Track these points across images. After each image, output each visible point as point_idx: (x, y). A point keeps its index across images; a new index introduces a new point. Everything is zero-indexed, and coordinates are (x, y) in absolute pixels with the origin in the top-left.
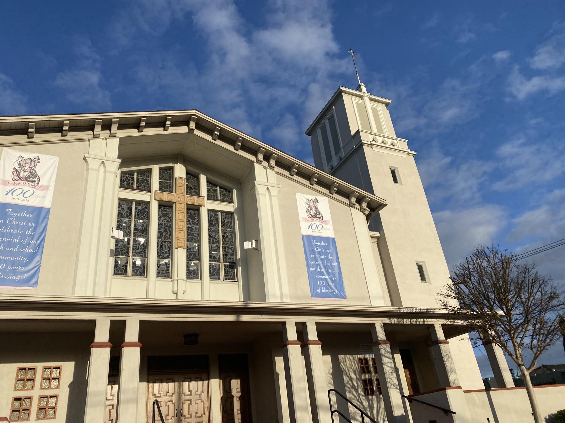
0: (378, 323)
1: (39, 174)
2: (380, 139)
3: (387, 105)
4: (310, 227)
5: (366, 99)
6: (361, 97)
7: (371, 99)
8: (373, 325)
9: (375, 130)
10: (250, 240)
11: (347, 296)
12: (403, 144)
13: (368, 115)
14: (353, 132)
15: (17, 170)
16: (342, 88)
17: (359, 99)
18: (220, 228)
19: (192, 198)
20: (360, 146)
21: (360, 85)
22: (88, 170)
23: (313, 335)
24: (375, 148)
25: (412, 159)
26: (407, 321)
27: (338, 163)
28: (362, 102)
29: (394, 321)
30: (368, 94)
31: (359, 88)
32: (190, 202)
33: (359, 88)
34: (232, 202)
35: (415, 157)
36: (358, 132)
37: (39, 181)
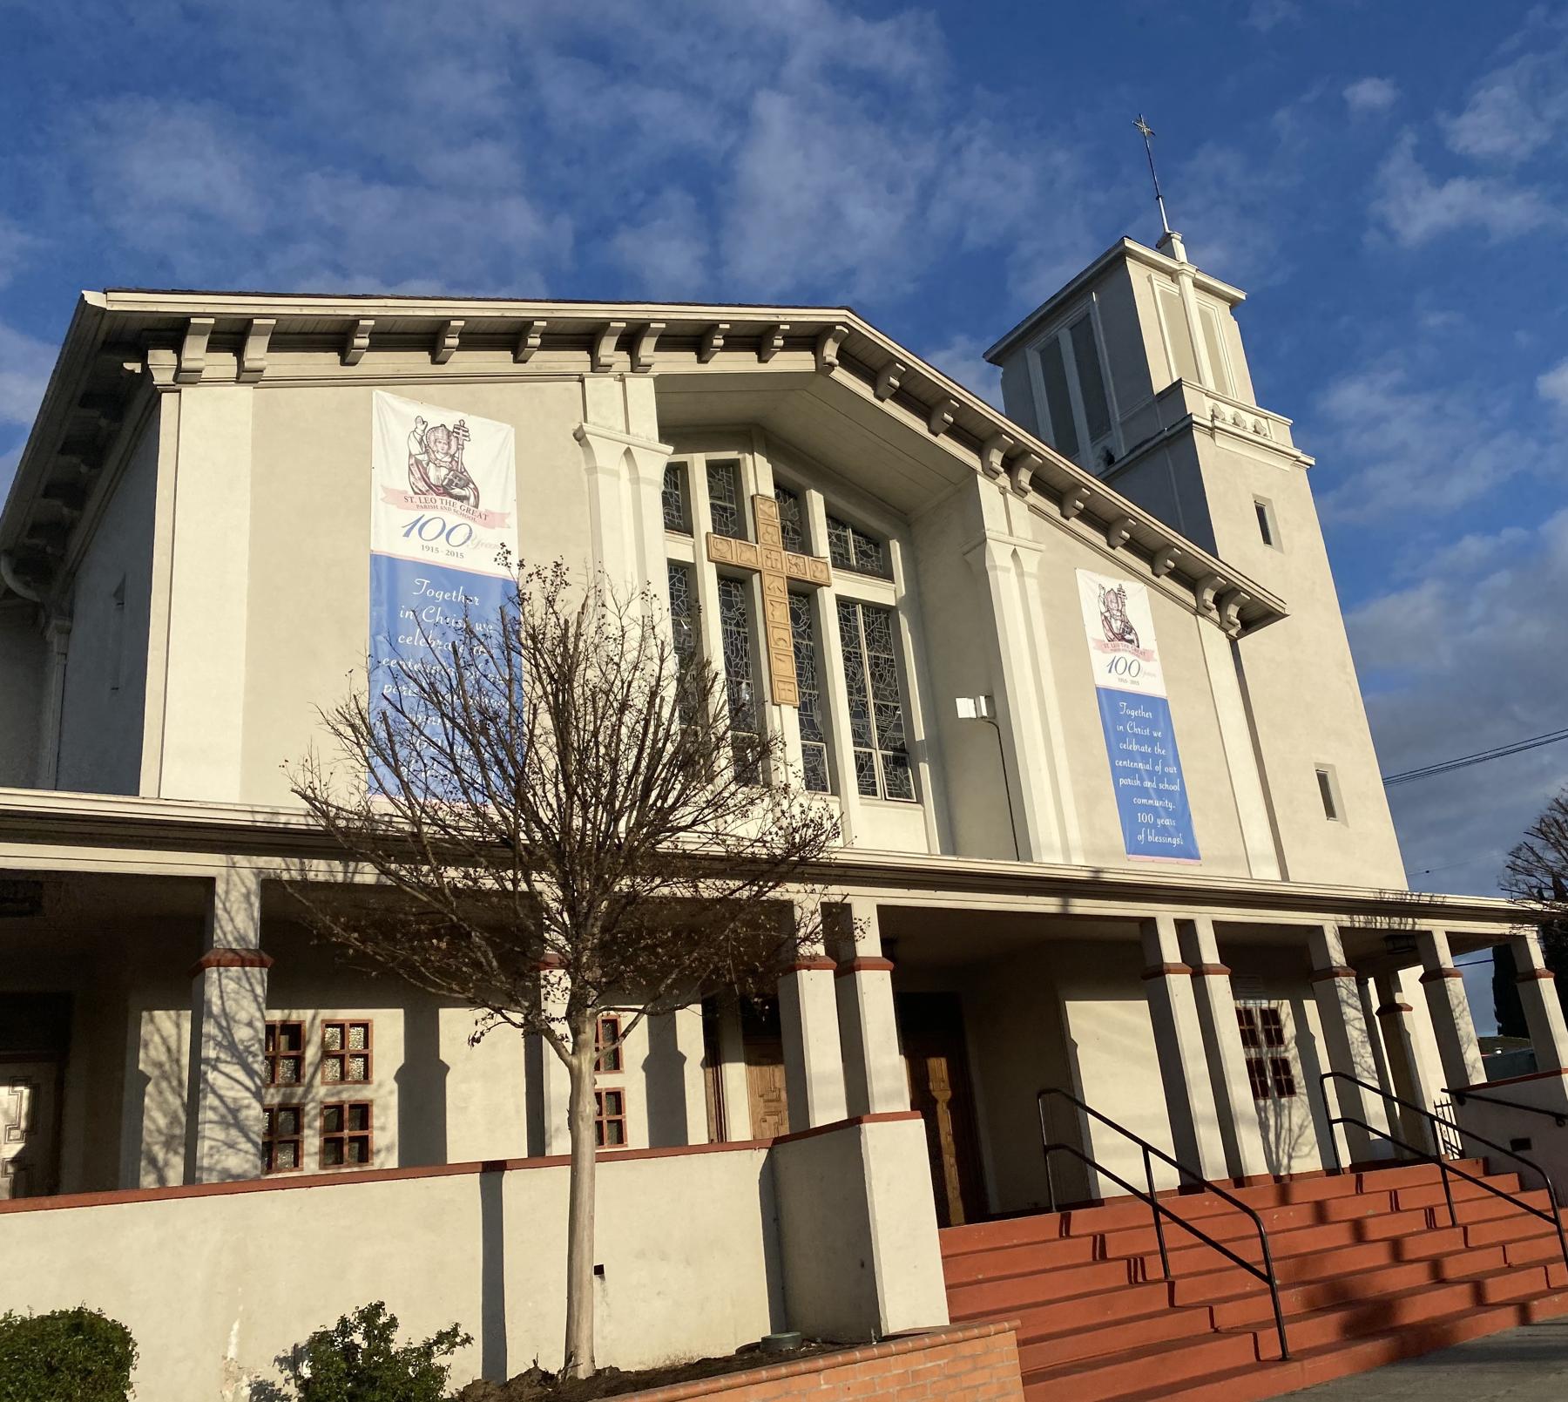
0: (1330, 924)
2: (1228, 412)
3: (1234, 304)
4: (1113, 665)
5: (1187, 282)
6: (1173, 275)
7: (1198, 285)
8: (1319, 930)
9: (1210, 384)
10: (974, 696)
11: (1202, 853)
12: (1278, 431)
13: (1188, 329)
14: (1160, 383)
16: (1128, 243)
17: (1166, 279)
18: (865, 653)
19: (800, 562)
20: (1186, 426)
21: (1168, 237)
23: (1210, 954)
24: (1221, 441)
25: (1302, 477)
26: (1382, 922)
27: (1136, 477)
28: (1175, 289)
29: (1360, 921)
30: (1191, 269)
31: (1164, 245)
33: (1164, 245)
34: (888, 576)
35: (1311, 470)
36: (1176, 387)
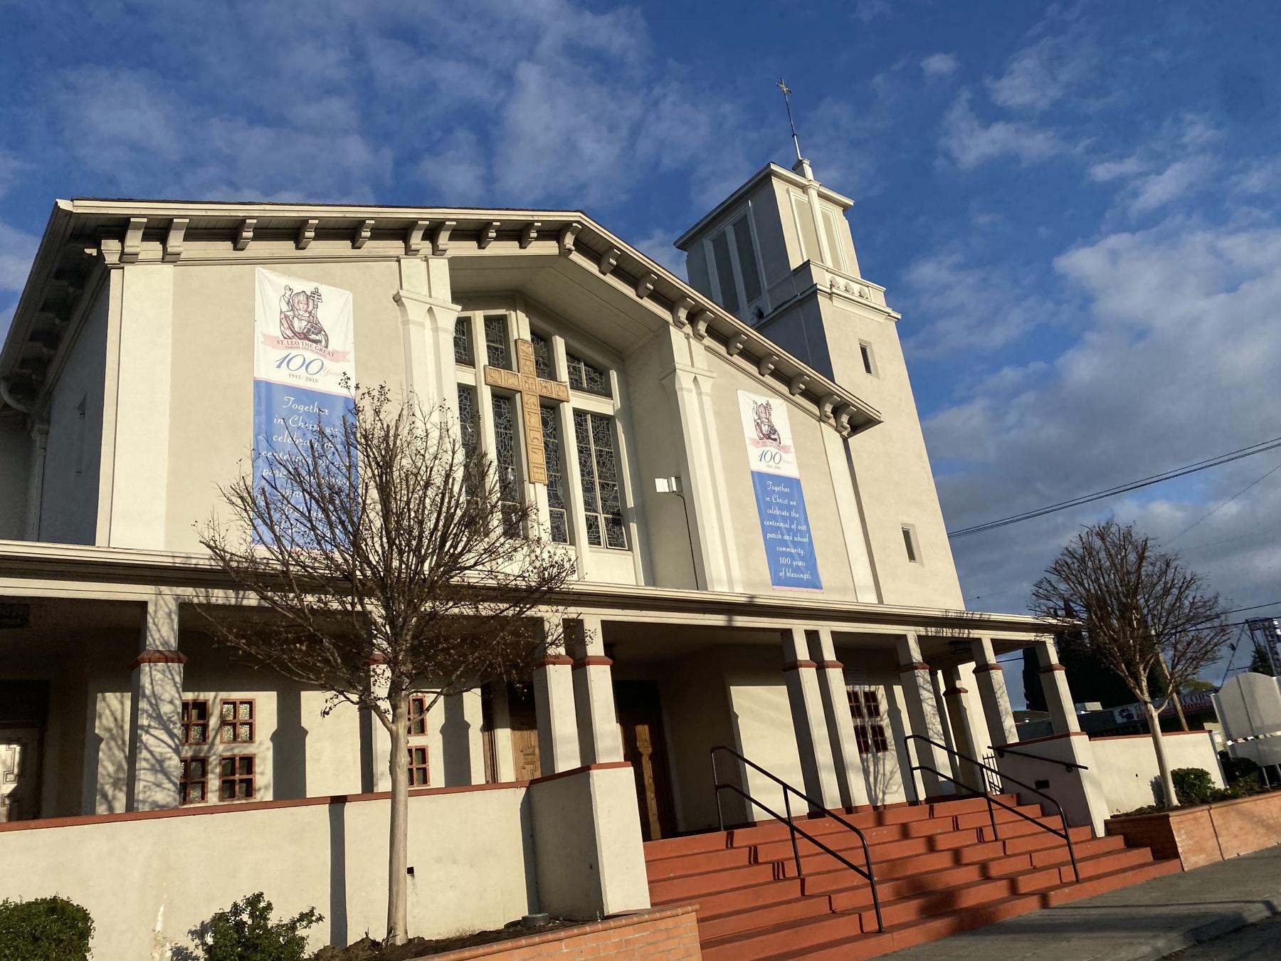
0: (911, 633)
1: (325, 324)
2: (841, 282)
3: (846, 209)
4: (763, 456)
5: (813, 193)
6: (804, 189)
7: (821, 195)
8: (904, 637)
9: (829, 264)
10: (667, 477)
12: (876, 295)
13: (814, 225)
14: (795, 263)
15: (286, 317)
16: (773, 167)
17: (799, 191)
18: (593, 448)
20: (813, 292)
21: (800, 163)
22: (406, 322)
26: (947, 632)
28: (805, 198)
29: (932, 631)
30: (816, 184)
31: (797, 168)
32: (545, 393)
33: (797, 168)
34: (609, 395)
35: (898, 322)
36: (806, 265)
37: (327, 341)
